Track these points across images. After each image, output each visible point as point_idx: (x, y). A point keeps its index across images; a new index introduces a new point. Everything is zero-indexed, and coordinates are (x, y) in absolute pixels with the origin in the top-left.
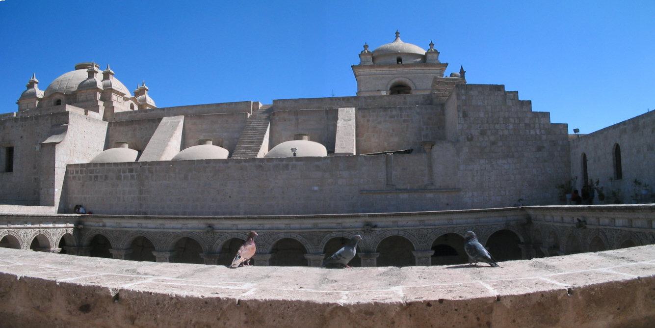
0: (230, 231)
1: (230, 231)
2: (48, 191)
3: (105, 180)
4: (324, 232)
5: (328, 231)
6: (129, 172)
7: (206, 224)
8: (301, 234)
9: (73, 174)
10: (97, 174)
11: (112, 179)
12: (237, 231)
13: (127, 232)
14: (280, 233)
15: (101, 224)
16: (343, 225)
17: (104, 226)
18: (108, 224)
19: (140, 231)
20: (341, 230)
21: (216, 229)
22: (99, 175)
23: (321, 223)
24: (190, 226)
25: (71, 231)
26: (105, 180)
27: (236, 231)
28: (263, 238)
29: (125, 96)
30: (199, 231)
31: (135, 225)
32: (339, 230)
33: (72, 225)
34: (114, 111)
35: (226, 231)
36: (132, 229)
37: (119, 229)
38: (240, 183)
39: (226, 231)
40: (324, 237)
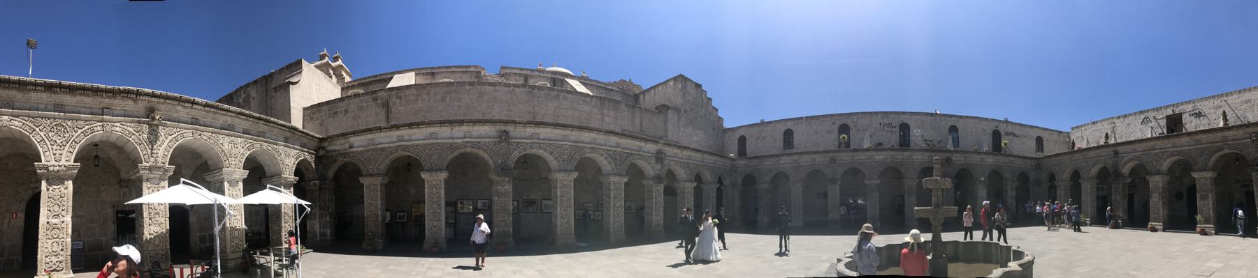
3: (345, 114)
6: (372, 101)
11: (353, 111)
13: (383, 149)
17: (351, 147)
19: (401, 146)
26: (345, 114)
31: (394, 139)
36: (392, 145)
37: (373, 147)
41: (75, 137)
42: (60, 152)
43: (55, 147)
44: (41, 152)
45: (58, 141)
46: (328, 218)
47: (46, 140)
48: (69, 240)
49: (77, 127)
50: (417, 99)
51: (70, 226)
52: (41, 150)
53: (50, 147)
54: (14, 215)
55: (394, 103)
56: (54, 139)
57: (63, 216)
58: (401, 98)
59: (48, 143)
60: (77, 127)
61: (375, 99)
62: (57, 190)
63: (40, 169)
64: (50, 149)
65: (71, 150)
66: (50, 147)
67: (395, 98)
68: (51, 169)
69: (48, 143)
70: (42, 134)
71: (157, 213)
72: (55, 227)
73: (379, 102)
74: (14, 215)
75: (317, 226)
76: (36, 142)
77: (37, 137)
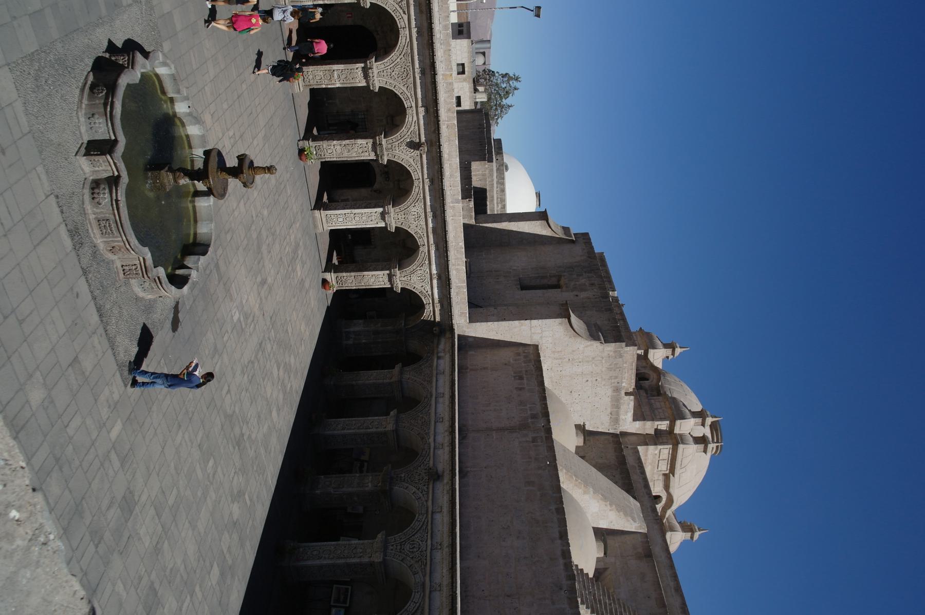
0: (430, 503)
1: (430, 503)
2: (493, 315)
7: (443, 472)
8: (420, 611)
9: (524, 352)
10: (525, 378)
12: (430, 513)
13: (430, 382)
14: (424, 576)
15: (441, 354)
18: (441, 362)
19: (431, 396)
21: (433, 483)
22: (525, 381)
24: (440, 452)
25: (427, 314)
26: (516, 388)
27: (430, 509)
28: (415, 550)
30: (431, 462)
31: (441, 390)
33: (438, 319)
34: (641, 445)
35: (430, 497)
38: (525, 558)
39: (430, 497)
41: (399, 85)
42: (385, 75)
43: (389, 70)
44: (384, 61)
45: (394, 73)
46: (364, 341)
47: (393, 64)
48: (324, 86)
49: (408, 87)
50: (531, 458)
51: (333, 86)
52: (386, 61)
53: (389, 67)
54: (350, 15)
56: (395, 69)
57: (339, 81)
58: (533, 442)
59: (391, 66)
60: (408, 87)
61: (534, 416)
62: (360, 73)
63: (370, 63)
64: (387, 68)
65: (388, 83)
66: (389, 67)
67: (534, 435)
68: (370, 71)
69: (391, 66)
70: (398, 60)
71: (349, 151)
72: (332, 76)
73: (530, 420)
74: (350, 15)
75: (357, 329)
76: (390, 57)
77: (395, 57)
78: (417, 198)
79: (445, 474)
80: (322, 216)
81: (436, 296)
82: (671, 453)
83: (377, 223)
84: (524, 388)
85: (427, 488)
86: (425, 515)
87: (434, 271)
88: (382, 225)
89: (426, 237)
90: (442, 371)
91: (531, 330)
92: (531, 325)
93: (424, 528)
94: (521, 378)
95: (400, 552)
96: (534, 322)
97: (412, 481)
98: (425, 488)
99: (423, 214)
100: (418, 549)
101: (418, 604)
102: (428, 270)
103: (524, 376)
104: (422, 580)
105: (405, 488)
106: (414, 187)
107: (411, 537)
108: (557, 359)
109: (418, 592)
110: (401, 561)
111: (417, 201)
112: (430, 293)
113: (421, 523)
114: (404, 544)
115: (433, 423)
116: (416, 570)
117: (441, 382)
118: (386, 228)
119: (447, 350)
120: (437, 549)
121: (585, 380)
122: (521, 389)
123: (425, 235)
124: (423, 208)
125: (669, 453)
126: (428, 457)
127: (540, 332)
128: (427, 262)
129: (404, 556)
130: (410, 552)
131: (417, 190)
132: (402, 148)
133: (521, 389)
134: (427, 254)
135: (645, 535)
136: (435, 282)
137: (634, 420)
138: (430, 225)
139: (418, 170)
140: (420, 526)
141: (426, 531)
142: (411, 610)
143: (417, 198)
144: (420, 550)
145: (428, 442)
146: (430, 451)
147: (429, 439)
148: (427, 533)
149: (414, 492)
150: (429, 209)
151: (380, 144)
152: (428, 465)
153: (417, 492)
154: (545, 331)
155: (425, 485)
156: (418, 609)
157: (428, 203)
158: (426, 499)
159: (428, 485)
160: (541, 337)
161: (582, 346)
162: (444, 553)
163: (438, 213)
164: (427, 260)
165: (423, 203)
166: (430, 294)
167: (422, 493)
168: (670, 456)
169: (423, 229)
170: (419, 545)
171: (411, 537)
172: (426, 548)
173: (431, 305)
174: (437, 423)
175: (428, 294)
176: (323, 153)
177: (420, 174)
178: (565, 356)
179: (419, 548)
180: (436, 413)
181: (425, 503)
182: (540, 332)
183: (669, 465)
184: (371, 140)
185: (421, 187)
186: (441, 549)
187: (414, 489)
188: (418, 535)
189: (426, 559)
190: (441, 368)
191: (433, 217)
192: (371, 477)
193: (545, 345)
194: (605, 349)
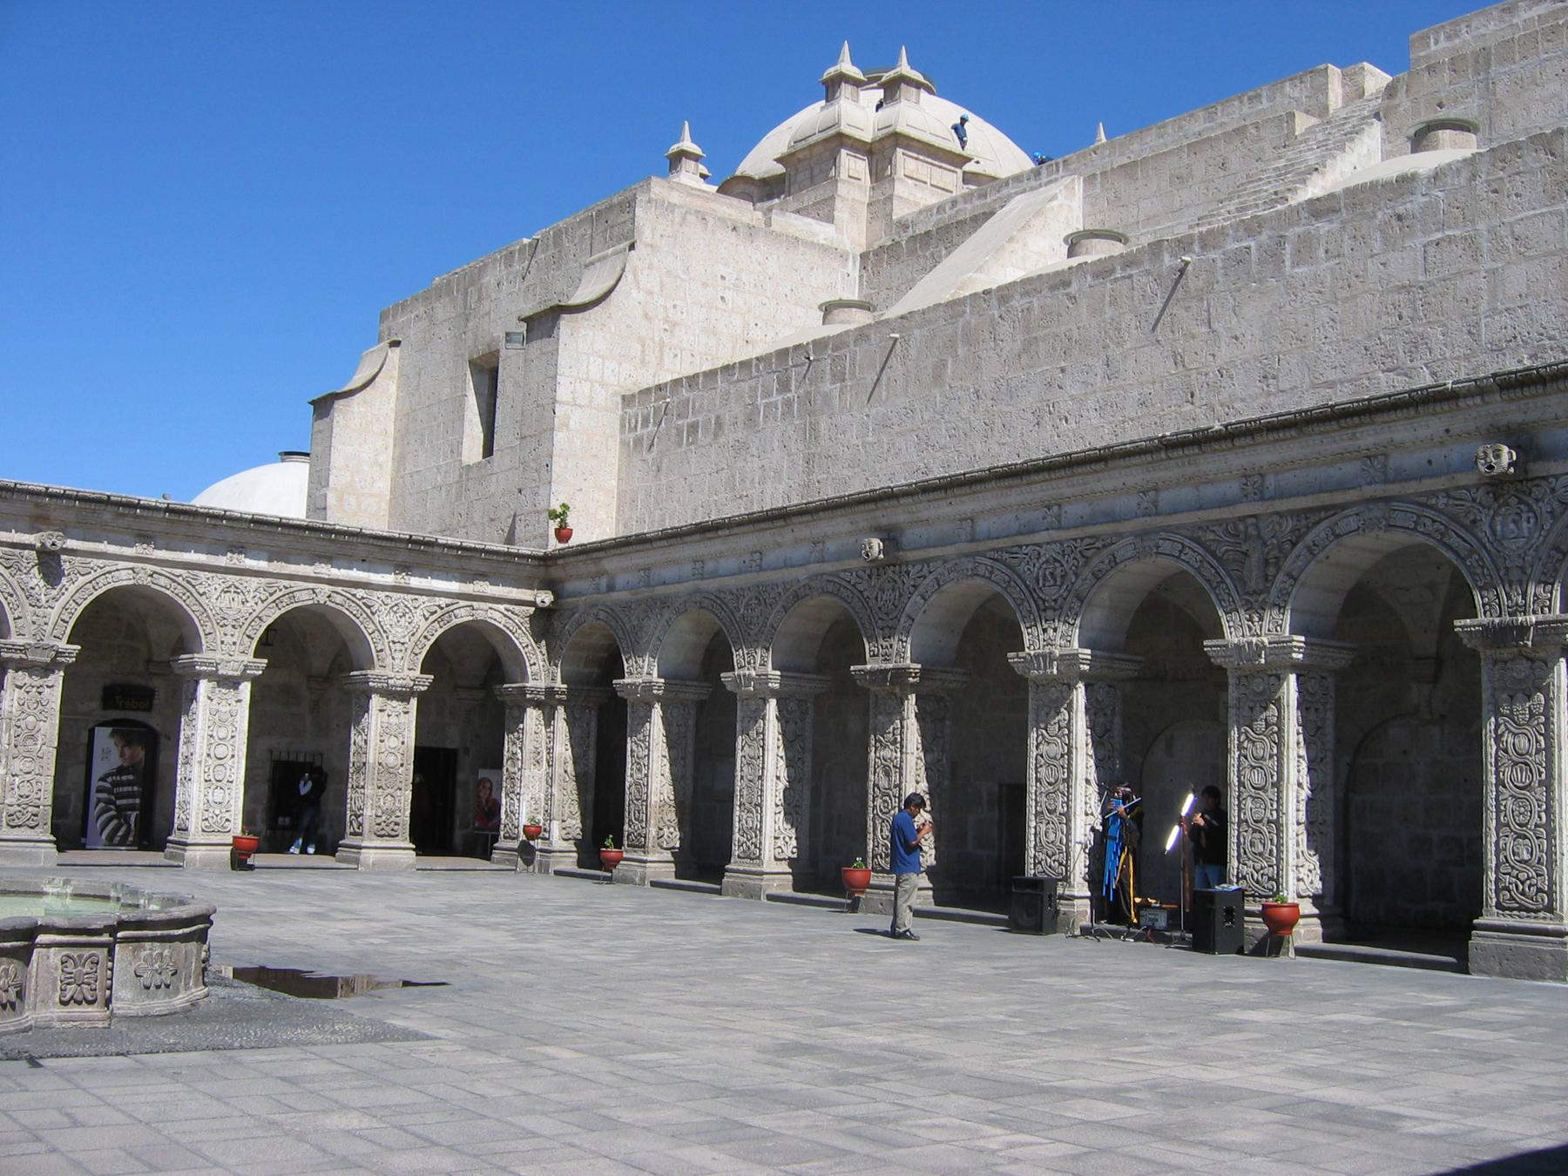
0: (949, 551)
1: (949, 551)
4: (1294, 513)
5: (1325, 508)
12: (973, 547)
14: (1120, 536)
16: (1392, 464)
18: (620, 580)
19: (698, 591)
20: (1379, 490)
23: (1276, 468)
27: (966, 547)
29: (969, 167)
32: (1368, 491)
37: (645, 593)
40: (1294, 544)
55: (827, 398)
78: (184, 583)
79: (884, 522)
80: (202, 842)
81: (454, 586)
82: (915, 155)
83: (239, 701)
84: (718, 417)
85: (914, 563)
86: (978, 559)
87: (389, 579)
88: (246, 688)
89: (292, 583)
90: (642, 573)
91: (581, 406)
92: (568, 403)
93: (1007, 555)
94: (693, 428)
95: (1061, 608)
96: (562, 393)
97: (896, 607)
98: (913, 571)
99: (228, 577)
100: (1057, 564)
101: (1187, 542)
102: (382, 595)
103: (689, 420)
104: (1130, 539)
105: (910, 622)
106: (153, 586)
107: (1027, 587)
108: (662, 359)
109: (1158, 547)
110: (1082, 602)
111: (194, 586)
112: (443, 601)
113: (998, 565)
114: (1044, 601)
115: (764, 577)
116: (1107, 561)
117: (667, 573)
118: (255, 681)
119: (592, 568)
120: (1060, 515)
121: (720, 304)
122: (719, 424)
123: (286, 583)
124: (214, 574)
125: (916, 159)
126: (842, 575)
127: (586, 387)
128: (360, 593)
129: (1071, 595)
130: (1062, 583)
131: (163, 581)
132: (43, 597)
133: (719, 424)
134: (339, 589)
135: (1090, 180)
136: (415, 582)
137: (830, 219)
138: (262, 565)
139: (107, 569)
140: (1003, 568)
141: (1016, 549)
142: (1199, 558)
143: (184, 583)
144: (1059, 558)
145: (806, 581)
146: (830, 574)
147: (799, 581)
148: (1021, 547)
149: (923, 597)
150: (222, 561)
151: (24, 649)
152: (861, 573)
153: (921, 589)
154: (587, 373)
155: (908, 573)
156: (1197, 541)
157: (202, 558)
158: (940, 562)
159: (907, 564)
160: (603, 385)
161: (634, 293)
162: (1068, 492)
163: (230, 536)
164: (354, 591)
165: (201, 574)
166: (449, 601)
167: (925, 577)
168: (921, 157)
169: (269, 585)
170: (1047, 562)
171: (1027, 587)
172: (1055, 542)
173: (476, 604)
174: (764, 566)
175: (447, 606)
176: (30, 809)
177: (122, 564)
178: (657, 339)
179: (1056, 560)
180: (740, 572)
181: (949, 565)
182: (586, 387)
183: (944, 165)
184: (11, 672)
185: (158, 569)
186: (1060, 506)
187: (916, 598)
188: (1022, 568)
189: (1082, 539)
190: (633, 578)
191: (240, 553)
192: (880, 717)
193: (622, 380)
194: (649, 241)
